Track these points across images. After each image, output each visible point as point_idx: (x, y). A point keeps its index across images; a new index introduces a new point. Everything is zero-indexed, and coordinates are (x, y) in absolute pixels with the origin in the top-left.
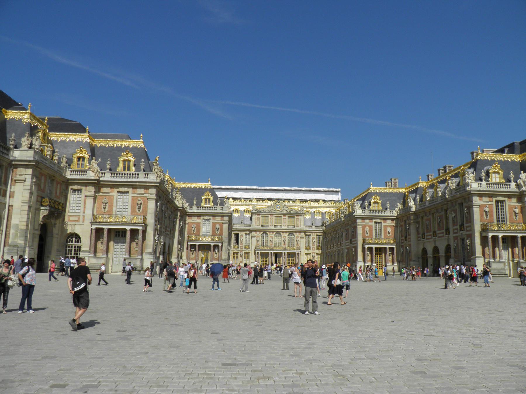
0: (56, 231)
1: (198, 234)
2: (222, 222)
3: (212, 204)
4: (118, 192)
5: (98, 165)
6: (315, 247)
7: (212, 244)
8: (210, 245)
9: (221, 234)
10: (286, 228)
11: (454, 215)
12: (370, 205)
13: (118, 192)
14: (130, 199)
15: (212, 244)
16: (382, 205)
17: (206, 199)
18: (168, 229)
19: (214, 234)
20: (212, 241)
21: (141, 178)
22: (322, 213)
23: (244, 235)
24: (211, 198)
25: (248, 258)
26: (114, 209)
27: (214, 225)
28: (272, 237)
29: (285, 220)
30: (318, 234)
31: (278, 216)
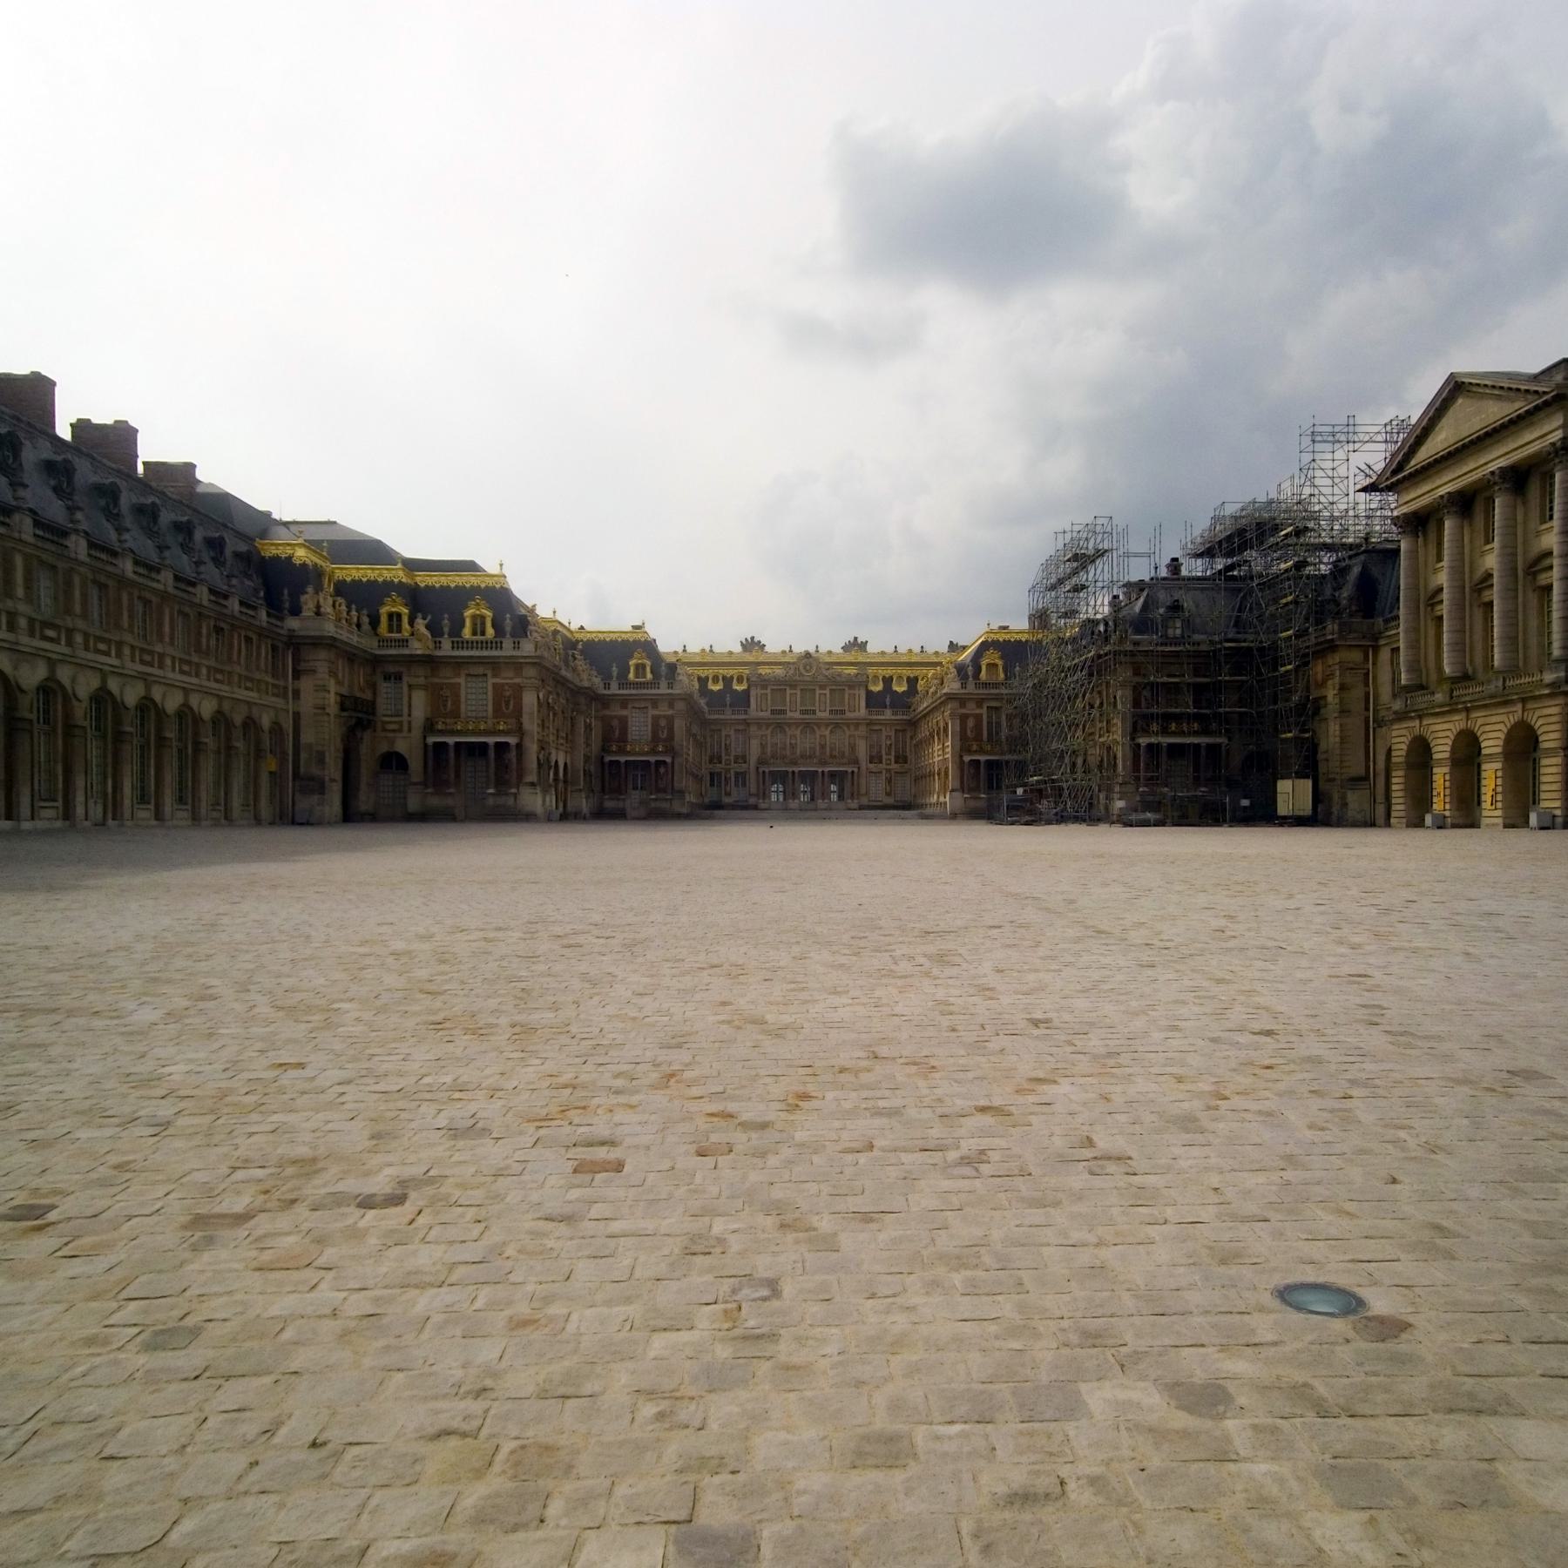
1: (623, 739)
2: (670, 712)
3: (649, 676)
5: (427, 627)
10: (826, 715)
12: (978, 670)
14: (490, 688)
15: (652, 759)
16: (1005, 671)
17: (637, 666)
19: (655, 738)
21: (507, 650)
22: (909, 679)
24: (648, 663)
25: (744, 784)
26: (463, 707)
27: (656, 719)
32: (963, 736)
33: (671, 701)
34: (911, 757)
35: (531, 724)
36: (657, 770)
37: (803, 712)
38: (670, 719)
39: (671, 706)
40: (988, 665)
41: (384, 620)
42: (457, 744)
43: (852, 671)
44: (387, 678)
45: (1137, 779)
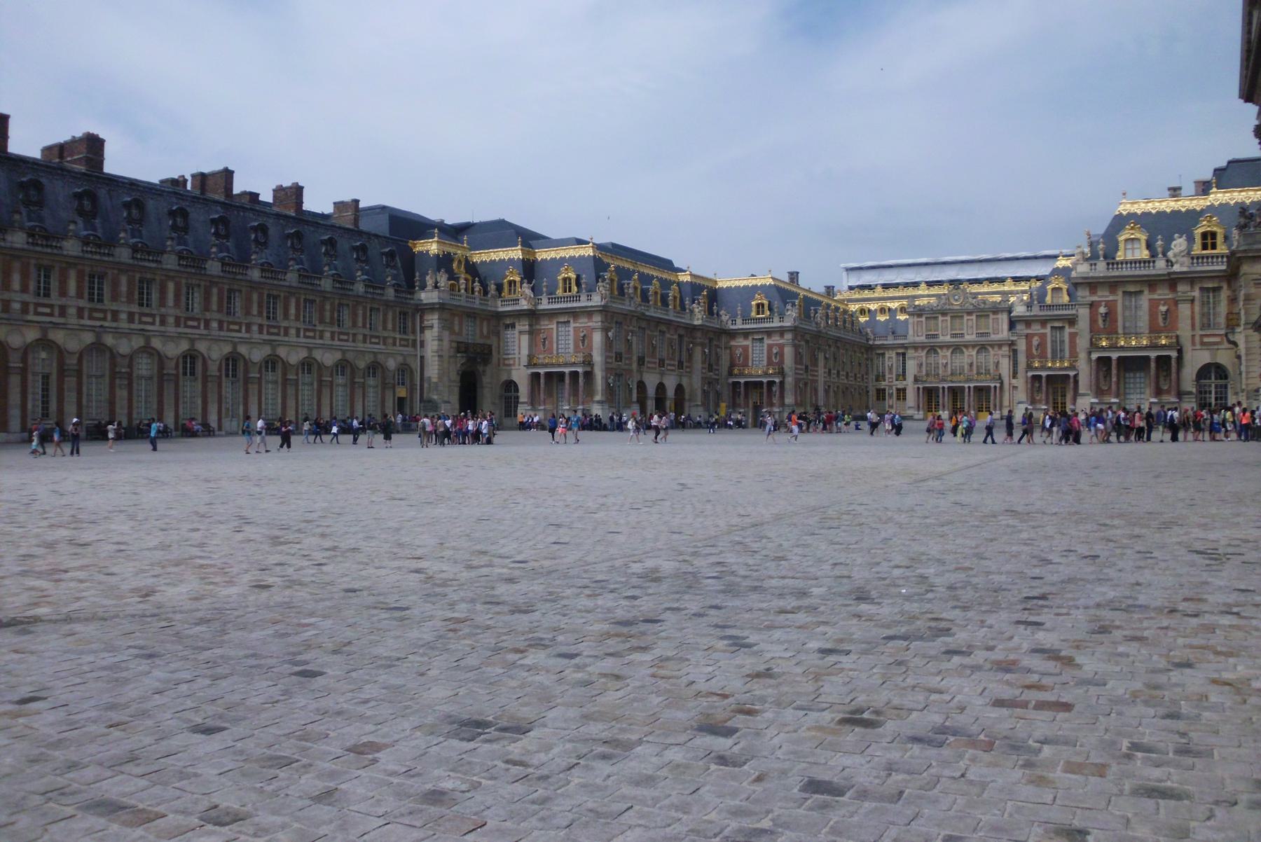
0: (486, 380)
1: (746, 365)
5: (533, 289)
9: (782, 361)
14: (571, 329)
15: (765, 380)
17: (758, 305)
19: (770, 363)
20: (766, 374)
21: (583, 303)
23: (894, 355)
24: (766, 302)
25: (905, 399)
27: (770, 347)
31: (957, 315)
33: (781, 331)
35: (597, 358)
37: (954, 335)
38: (781, 347)
40: (1053, 289)
41: (506, 287)
42: (547, 374)
43: (998, 298)
44: (507, 326)
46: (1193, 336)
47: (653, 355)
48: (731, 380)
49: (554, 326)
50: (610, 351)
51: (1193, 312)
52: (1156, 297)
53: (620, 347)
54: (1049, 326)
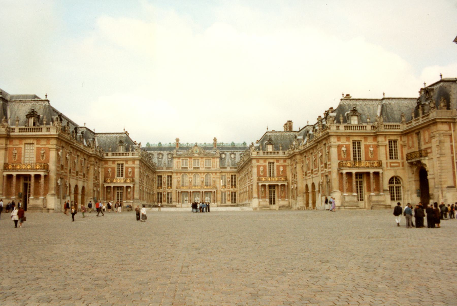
1: (113, 177)
2: (133, 166)
4: (25, 144)
6: (230, 186)
7: (125, 185)
8: (123, 187)
10: (204, 169)
11: (320, 154)
13: (25, 144)
14: (35, 149)
18: (79, 173)
19: (127, 177)
20: (125, 182)
23: (166, 177)
26: (23, 158)
28: (191, 178)
29: (202, 163)
30: (233, 174)
32: (259, 175)
33: (134, 160)
34: (238, 186)
35: (52, 167)
36: (127, 190)
38: (133, 168)
39: (134, 163)
45: (341, 190)
46: (387, 163)
47: (74, 169)
48: (105, 185)
49: (22, 146)
50: (59, 164)
51: (386, 151)
52: (367, 143)
53: (63, 162)
54: (268, 161)
